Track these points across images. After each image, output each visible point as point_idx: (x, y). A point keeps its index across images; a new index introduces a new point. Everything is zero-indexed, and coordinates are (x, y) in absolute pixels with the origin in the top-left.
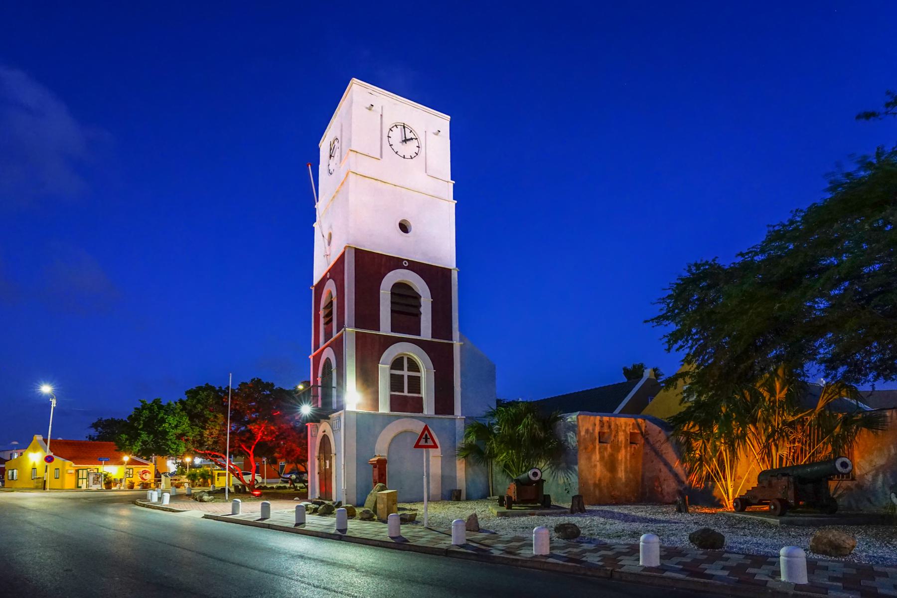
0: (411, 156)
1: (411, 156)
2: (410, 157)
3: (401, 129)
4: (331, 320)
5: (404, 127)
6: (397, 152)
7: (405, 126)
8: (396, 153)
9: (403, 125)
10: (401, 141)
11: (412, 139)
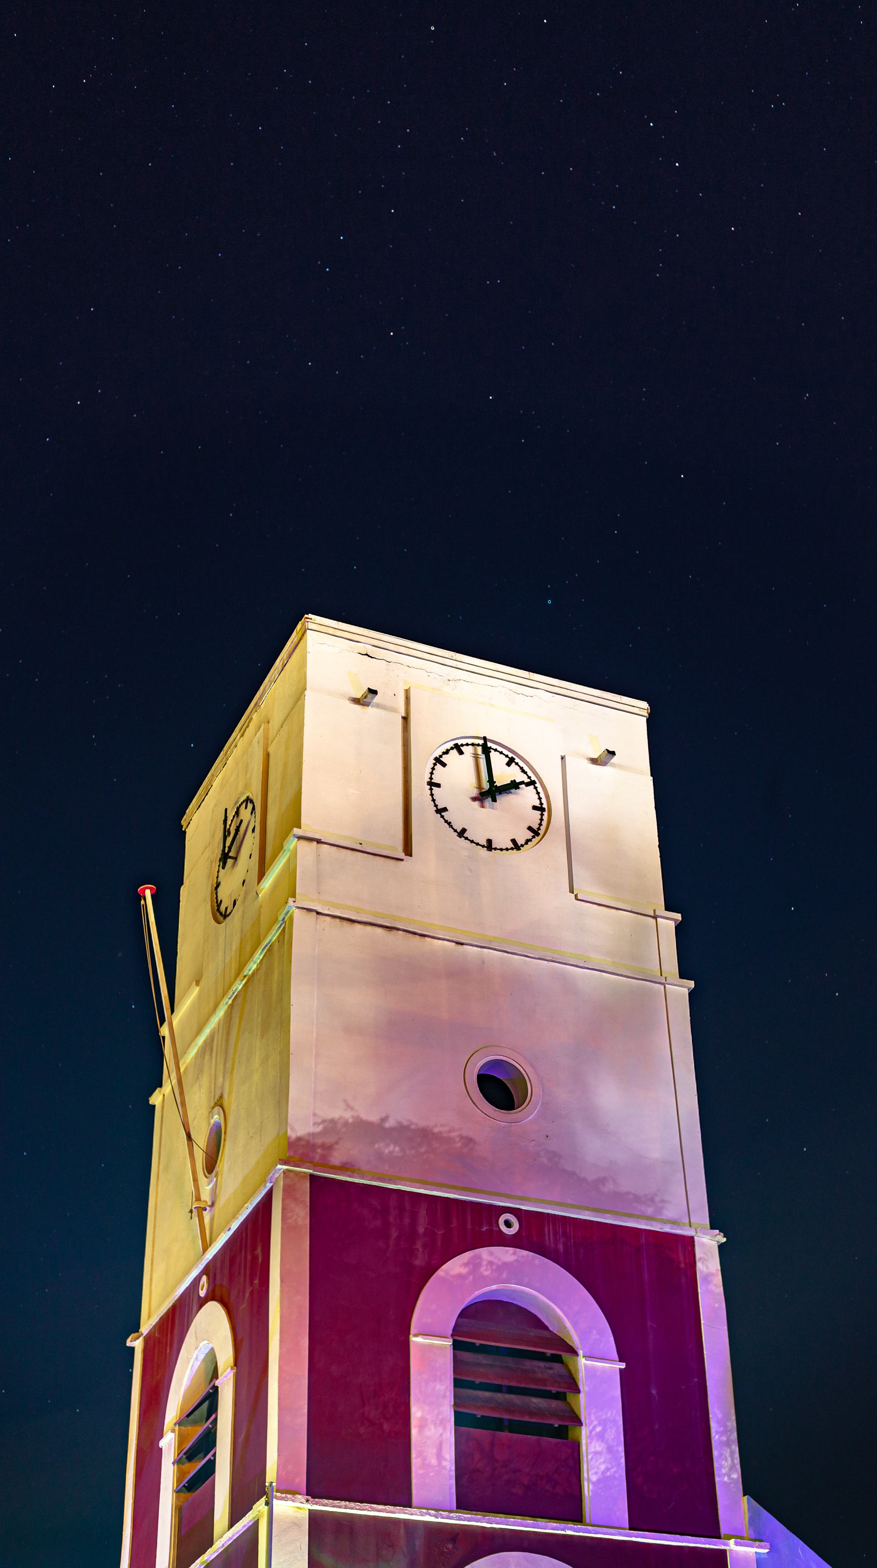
0: (514, 841)
1: (514, 841)
2: (511, 845)
3: (476, 757)
4: (209, 1469)
5: (486, 750)
6: (464, 830)
7: (489, 744)
8: (462, 833)
9: (481, 742)
10: (475, 793)
11: (514, 785)
